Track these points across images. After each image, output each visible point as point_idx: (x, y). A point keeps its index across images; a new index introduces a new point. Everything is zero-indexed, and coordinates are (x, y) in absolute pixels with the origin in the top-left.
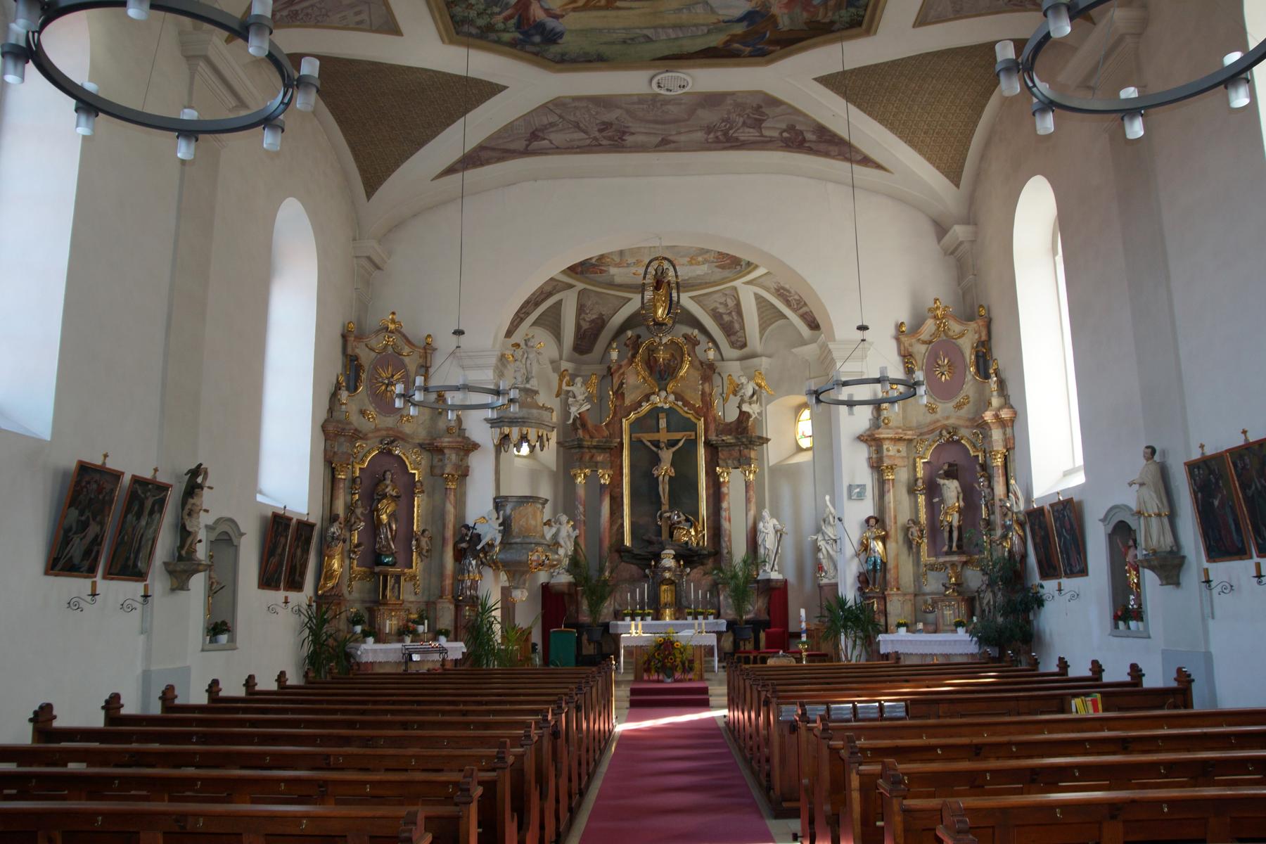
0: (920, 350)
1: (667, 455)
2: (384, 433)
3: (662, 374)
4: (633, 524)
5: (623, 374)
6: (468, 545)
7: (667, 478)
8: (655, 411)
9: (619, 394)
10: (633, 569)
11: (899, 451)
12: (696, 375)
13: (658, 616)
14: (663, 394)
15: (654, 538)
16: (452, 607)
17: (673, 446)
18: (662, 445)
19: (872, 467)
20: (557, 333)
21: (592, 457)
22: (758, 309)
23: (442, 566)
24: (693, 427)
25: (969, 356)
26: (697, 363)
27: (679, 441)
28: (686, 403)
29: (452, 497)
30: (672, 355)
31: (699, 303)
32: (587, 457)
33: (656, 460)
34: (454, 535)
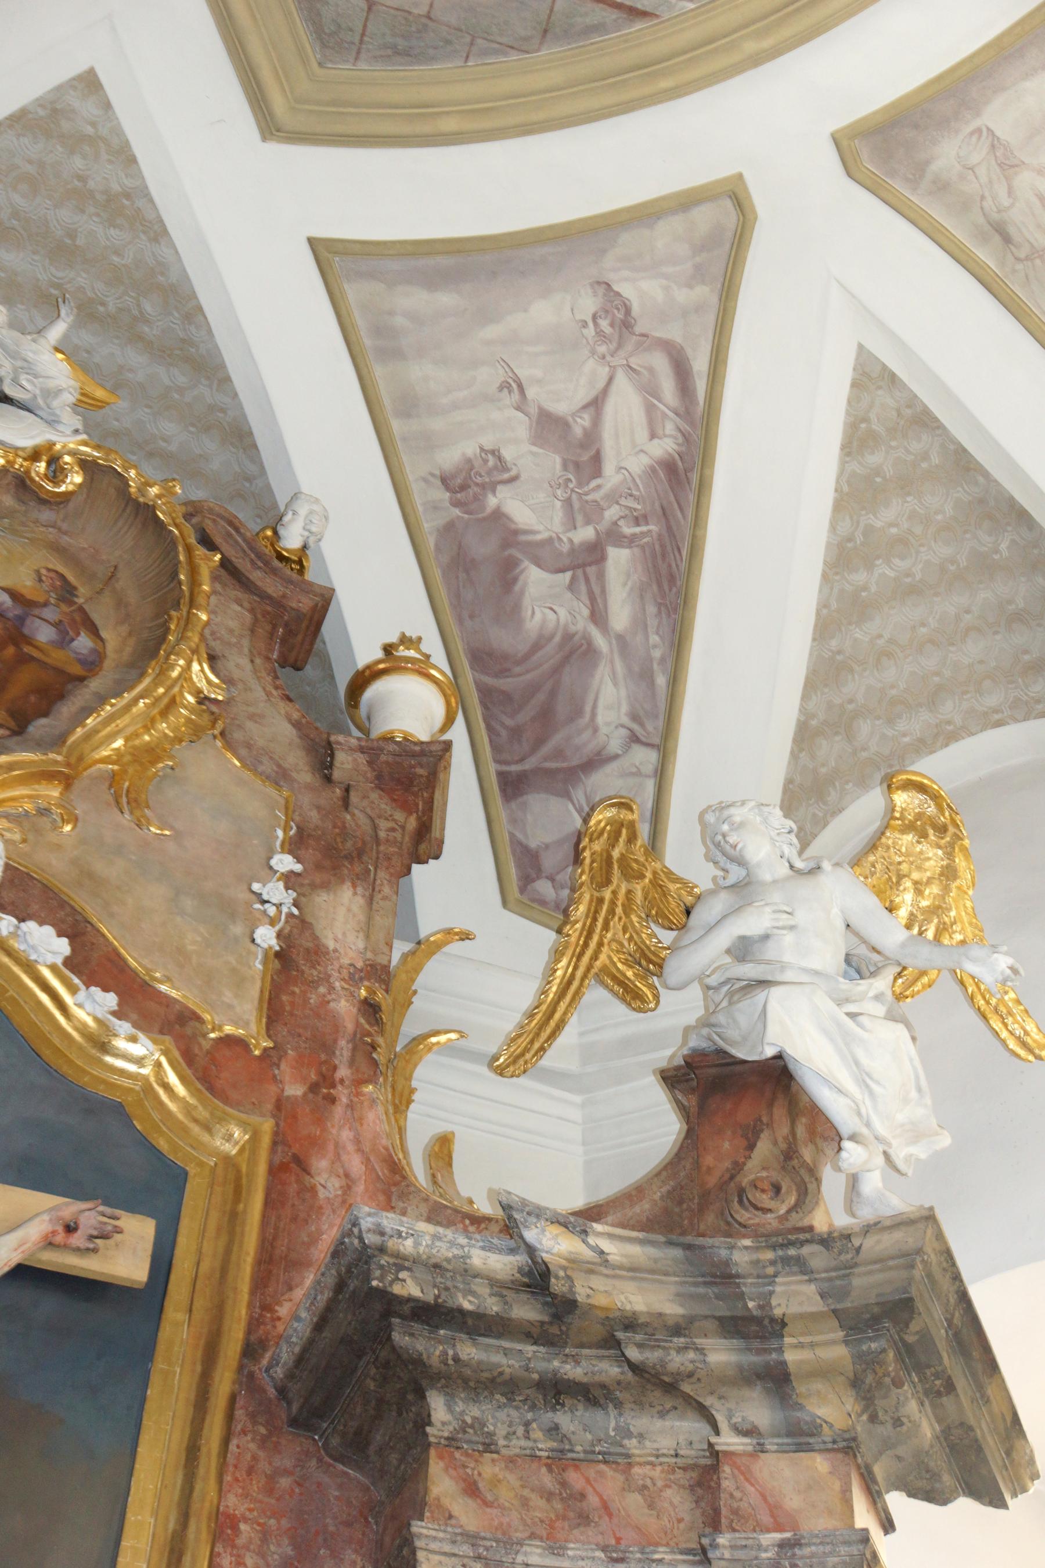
22: (842, 558)
31: (367, 349)
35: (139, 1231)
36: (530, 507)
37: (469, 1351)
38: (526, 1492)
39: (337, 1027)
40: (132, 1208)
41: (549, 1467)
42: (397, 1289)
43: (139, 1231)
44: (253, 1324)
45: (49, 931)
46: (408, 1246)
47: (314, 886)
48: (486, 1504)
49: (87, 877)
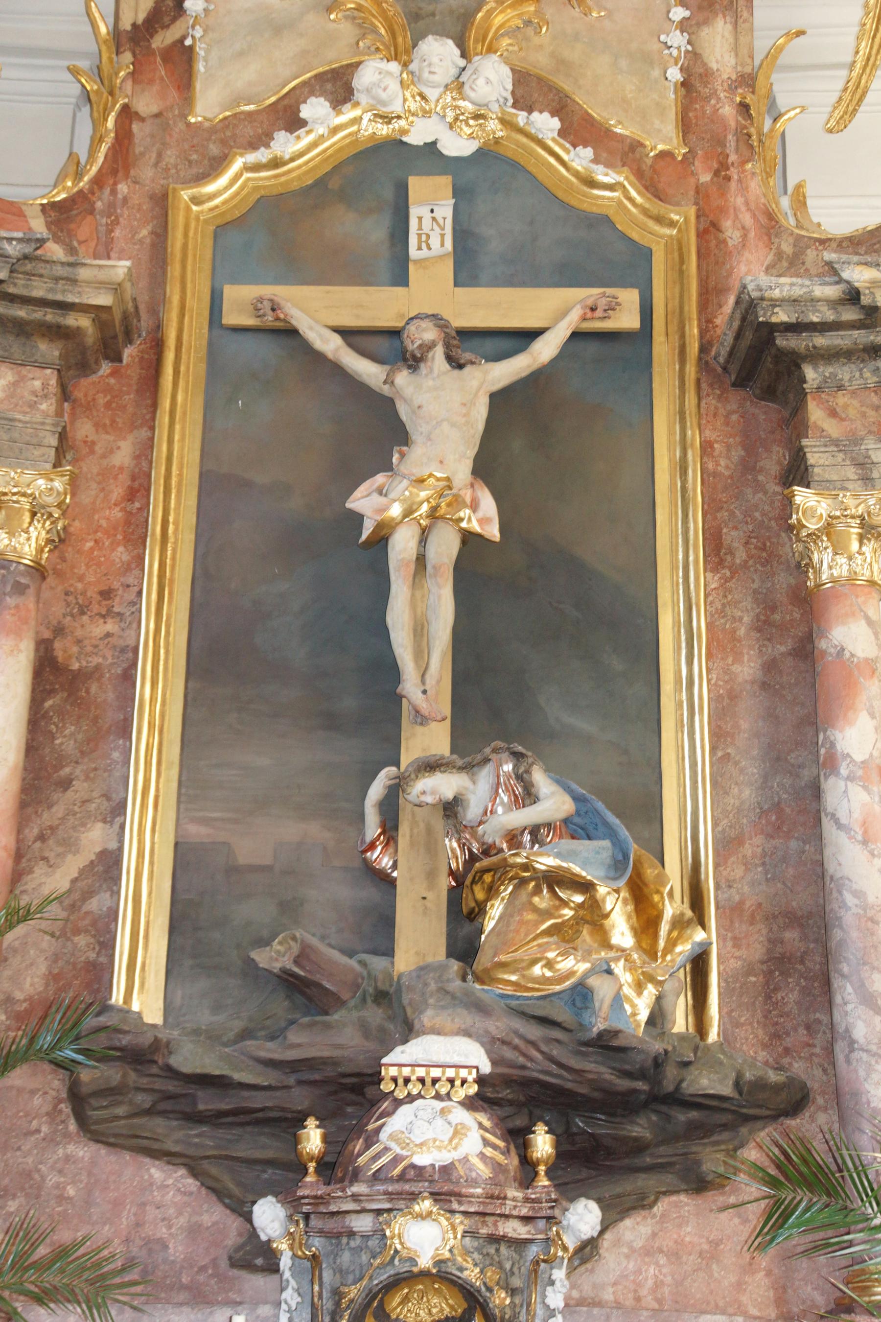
4: (186, 857)
7: (445, 548)
8: (382, 170)
14: (439, 53)
15: (338, 962)
28: (579, 128)
33: (380, 433)
37: (821, 341)
38: (864, 409)
39: (725, 128)
40: (624, 285)
41: (876, 392)
42: (774, 319)
43: (630, 297)
44: (702, 333)
45: (546, 115)
46: (777, 293)
47: (699, 25)
48: (842, 420)
49: (562, 64)
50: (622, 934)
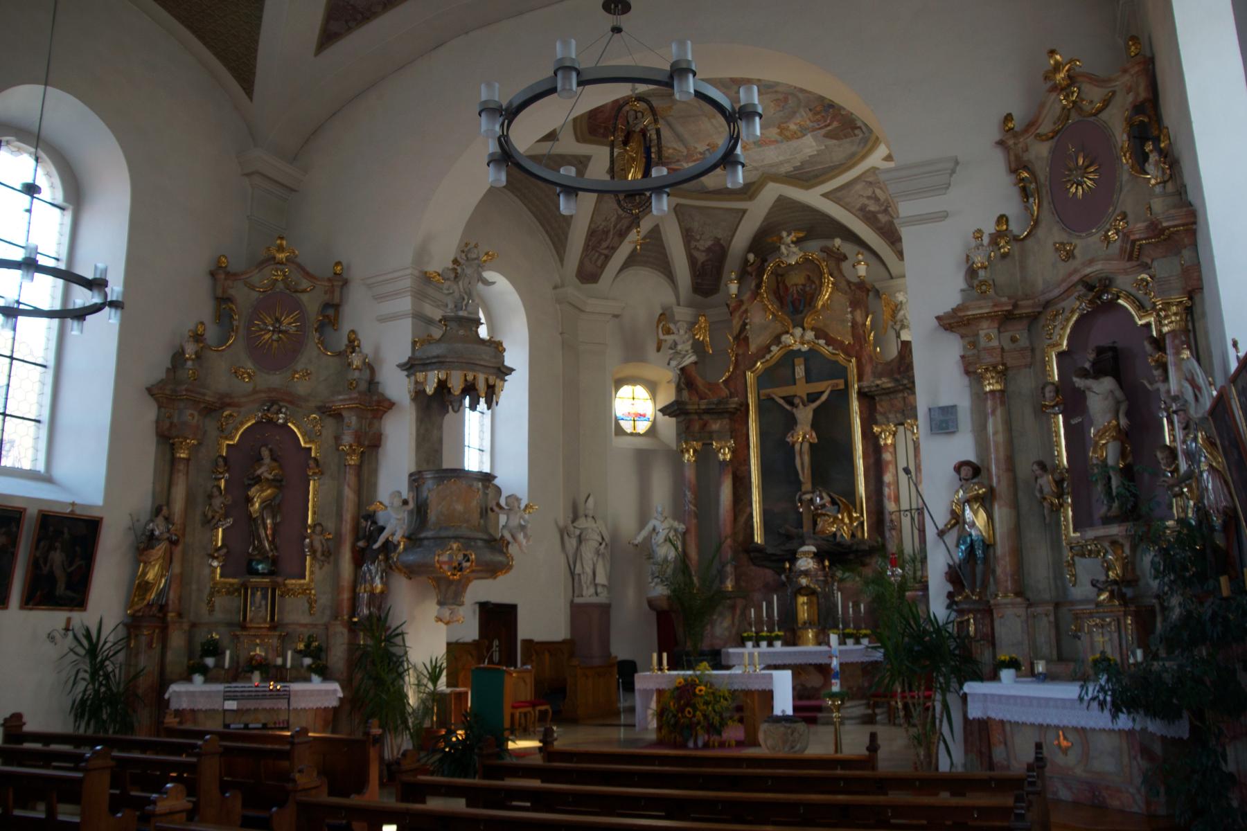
0: (1040, 151)
1: (804, 415)
2: (263, 395)
3: (796, 304)
4: (765, 513)
5: (746, 311)
6: (368, 543)
7: (806, 446)
8: (790, 356)
9: (742, 338)
10: (769, 574)
11: (1013, 340)
12: (843, 300)
13: (792, 639)
14: (798, 331)
16: (345, 631)
17: (813, 401)
18: (797, 401)
19: (967, 373)
20: (668, 272)
21: (705, 425)
23: (336, 575)
24: (842, 372)
25: (1121, 138)
26: (843, 285)
27: (822, 393)
29: (351, 478)
30: (809, 277)
31: (838, 201)
32: (696, 426)
33: (791, 422)
34: (356, 528)
35: (841, 381)
36: (873, 207)
43: (841, 381)
50: (846, 520)
